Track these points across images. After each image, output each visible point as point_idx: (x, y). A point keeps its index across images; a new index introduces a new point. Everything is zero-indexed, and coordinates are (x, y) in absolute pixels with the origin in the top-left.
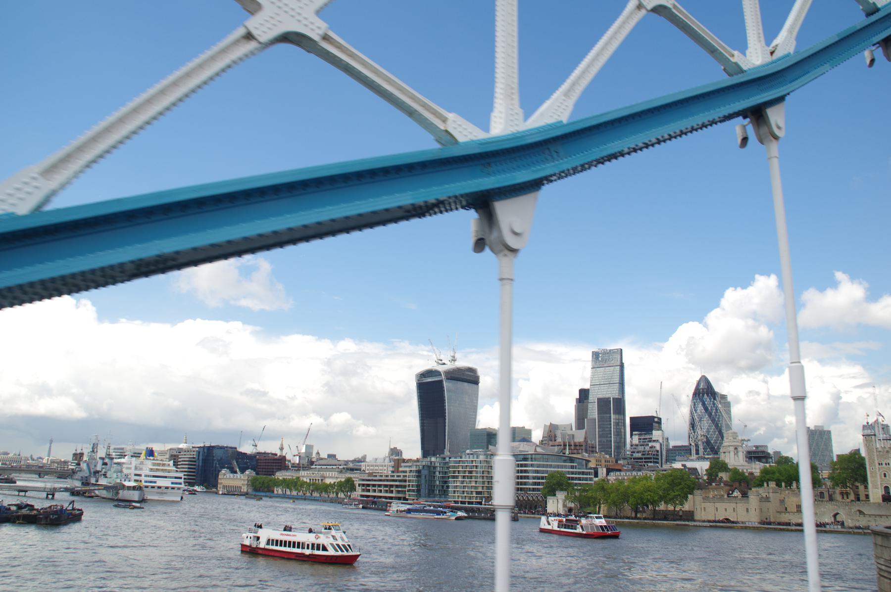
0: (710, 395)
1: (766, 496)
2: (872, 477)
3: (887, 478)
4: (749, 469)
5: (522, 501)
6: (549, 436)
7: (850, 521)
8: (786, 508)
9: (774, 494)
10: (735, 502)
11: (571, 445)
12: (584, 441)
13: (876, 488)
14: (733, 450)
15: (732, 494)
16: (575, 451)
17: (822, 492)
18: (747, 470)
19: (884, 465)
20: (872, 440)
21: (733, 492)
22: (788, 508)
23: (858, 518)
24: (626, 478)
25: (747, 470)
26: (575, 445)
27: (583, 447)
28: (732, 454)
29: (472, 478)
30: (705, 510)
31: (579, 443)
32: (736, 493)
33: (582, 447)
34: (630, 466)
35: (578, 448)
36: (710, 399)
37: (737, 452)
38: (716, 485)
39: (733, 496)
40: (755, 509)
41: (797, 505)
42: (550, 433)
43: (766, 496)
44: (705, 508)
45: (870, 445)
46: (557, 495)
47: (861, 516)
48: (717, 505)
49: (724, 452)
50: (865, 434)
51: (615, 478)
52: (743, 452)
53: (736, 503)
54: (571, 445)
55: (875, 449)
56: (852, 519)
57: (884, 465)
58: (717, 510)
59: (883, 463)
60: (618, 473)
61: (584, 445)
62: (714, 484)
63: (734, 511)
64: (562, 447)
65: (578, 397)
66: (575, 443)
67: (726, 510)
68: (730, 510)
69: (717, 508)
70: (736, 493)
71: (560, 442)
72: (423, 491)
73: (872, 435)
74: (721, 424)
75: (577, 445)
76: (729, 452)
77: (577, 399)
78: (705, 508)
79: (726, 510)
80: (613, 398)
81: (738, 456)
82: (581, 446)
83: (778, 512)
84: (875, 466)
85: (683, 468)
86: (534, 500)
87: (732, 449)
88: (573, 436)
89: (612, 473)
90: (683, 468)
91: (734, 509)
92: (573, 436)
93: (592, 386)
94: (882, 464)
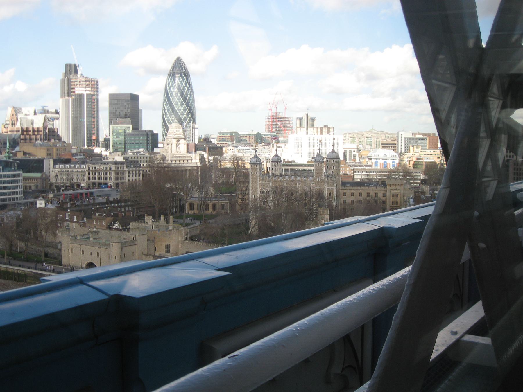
0: (183, 75)
6: (12, 120)
8: (156, 248)
9: (141, 237)
11: (30, 131)
15: (114, 225)
21: (114, 223)
26: (34, 131)
28: (174, 145)
32: (117, 225)
33: (40, 133)
34: (82, 154)
38: (98, 215)
40: (116, 256)
41: (166, 245)
44: (72, 249)
45: (254, 173)
48: (83, 247)
50: (252, 162)
51: (59, 170)
52: (185, 144)
55: (258, 177)
58: (83, 253)
60: (62, 166)
61: (43, 131)
65: (64, 72)
69: (83, 251)
70: (117, 225)
71: (18, 128)
73: (258, 164)
76: (172, 144)
77: (63, 73)
78: (72, 249)
82: (39, 131)
83: (145, 255)
85: (124, 160)
87: (175, 141)
89: (57, 166)
90: (124, 160)
91: (98, 253)
92: (32, 121)
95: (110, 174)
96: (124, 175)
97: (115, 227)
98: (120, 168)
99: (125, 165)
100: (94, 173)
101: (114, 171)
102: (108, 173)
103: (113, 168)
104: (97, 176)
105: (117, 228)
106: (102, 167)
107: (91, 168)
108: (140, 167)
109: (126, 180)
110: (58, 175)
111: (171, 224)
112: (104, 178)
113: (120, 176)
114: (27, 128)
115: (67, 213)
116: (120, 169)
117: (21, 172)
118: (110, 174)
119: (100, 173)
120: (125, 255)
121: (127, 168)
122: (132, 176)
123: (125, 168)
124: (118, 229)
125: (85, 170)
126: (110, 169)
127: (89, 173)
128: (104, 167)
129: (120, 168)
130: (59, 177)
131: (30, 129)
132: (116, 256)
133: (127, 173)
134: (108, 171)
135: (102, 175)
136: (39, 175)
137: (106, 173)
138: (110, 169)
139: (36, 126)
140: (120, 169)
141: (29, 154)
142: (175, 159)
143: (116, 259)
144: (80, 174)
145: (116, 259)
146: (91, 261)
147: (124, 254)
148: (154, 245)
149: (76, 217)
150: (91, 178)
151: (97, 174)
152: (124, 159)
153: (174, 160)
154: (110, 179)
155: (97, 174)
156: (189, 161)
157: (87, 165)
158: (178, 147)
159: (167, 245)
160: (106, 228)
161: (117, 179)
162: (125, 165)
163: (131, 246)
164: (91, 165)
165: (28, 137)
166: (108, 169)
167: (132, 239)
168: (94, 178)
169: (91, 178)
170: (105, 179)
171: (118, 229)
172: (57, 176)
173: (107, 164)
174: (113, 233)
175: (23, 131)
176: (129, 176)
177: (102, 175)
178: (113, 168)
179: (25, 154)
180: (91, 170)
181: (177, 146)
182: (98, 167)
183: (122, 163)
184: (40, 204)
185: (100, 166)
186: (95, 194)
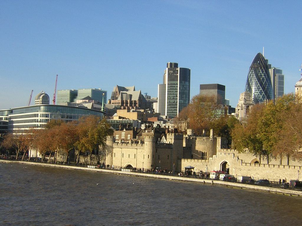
1: (170, 142)
7: (234, 169)
27: (137, 105)
40: (149, 155)
43: (170, 142)
49: (239, 110)
54: (127, 103)
56: (236, 168)
58: (123, 157)
63: (135, 157)
64: (120, 104)
67: (129, 155)
68: (132, 157)
69: (123, 154)
74: (269, 91)
78: (115, 154)
79: (129, 155)
91: (135, 155)
97: (161, 143)
107: (170, 127)
111: (211, 136)
115: (124, 133)
120: (160, 157)
132: (149, 155)
141: (123, 118)
143: (148, 158)
145: (148, 158)
147: (159, 156)
148: (191, 152)
157: (167, 124)
159: (203, 152)
163: (167, 149)
164: (170, 124)
167: (169, 143)
179: (120, 118)
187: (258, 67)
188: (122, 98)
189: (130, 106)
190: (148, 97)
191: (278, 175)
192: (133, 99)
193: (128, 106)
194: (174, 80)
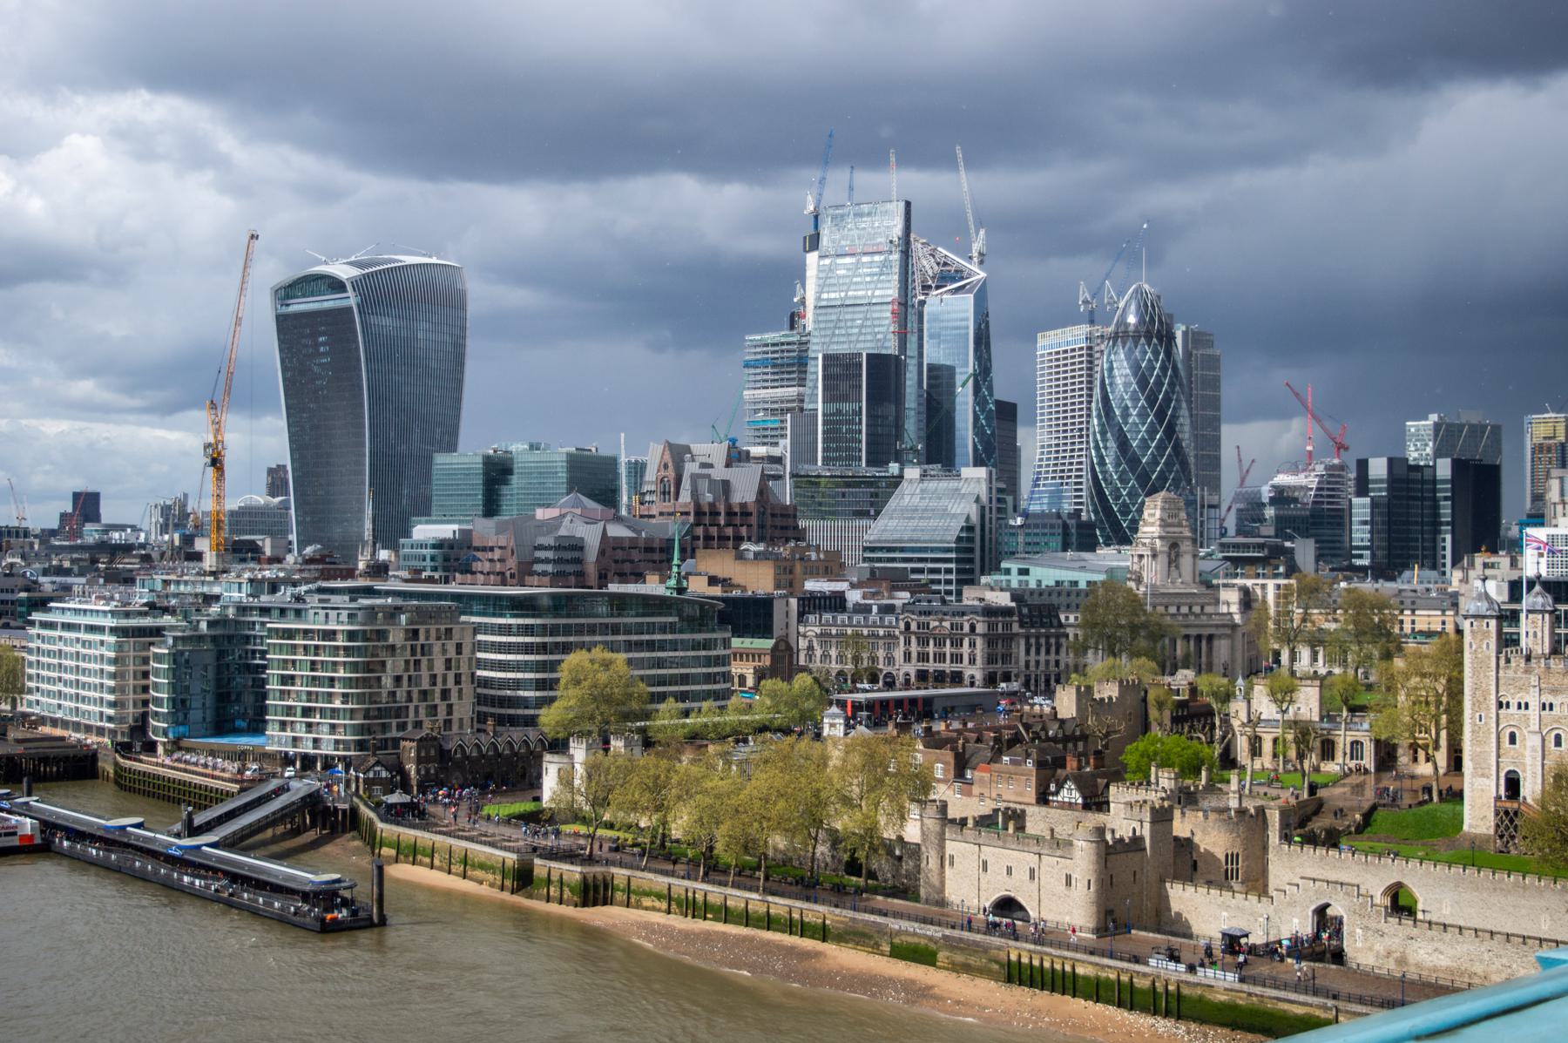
0: (1155, 340)
1: (1134, 830)
2: (1476, 741)
3: (1517, 746)
4: (1209, 604)
5: (478, 759)
6: (662, 481)
7: (1359, 931)
8: (1195, 862)
10: (1036, 849)
11: (718, 514)
12: (757, 501)
13: (1483, 775)
14: (1166, 549)
15: (1057, 793)
16: (729, 531)
17: (1357, 742)
18: (1202, 608)
19: (1513, 709)
20: (1488, 632)
21: (1060, 787)
22: (1199, 864)
23: (1382, 926)
24: (849, 631)
25: (1202, 608)
26: (730, 513)
27: (754, 520)
29: (333, 686)
30: (952, 864)
31: (743, 505)
32: (1070, 793)
35: (738, 520)
36: (1156, 353)
37: (1178, 555)
39: (1060, 799)
41: (1227, 856)
42: (662, 473)
43: (1134, 830)
46: (572, 751)
47: (1390, 919)
48: (989, 852)
51: (818, 630)
53: (1040, 855)
54: (715, 514)
56: (1366, 929)
57: (1513, 709)
58: (985, 869)
59: (1511, 701)
60: (827, 616)
62: (1006, 758)
63: (1032, 877)
64: (691, 519)
66: (729, 507)
67: (1009, 871)
68: (1021, 875)
69: (985, 863)
71: (686, 505)
72: (196, 715)
75: (736, 514)
78: (952, 857)
79: (1009, 871)
80: (868, 355)
81: (1177, 567)
82: (745, 513)
84: (1488, 709)
85: (1013, 604)
86: (516, 754)
88: (726, 485)
89: (811, 618)
90: (1013, 604)
91: (1032, 871)
92: (726, 485)
93: (819, 311)
94: (1508, 703)
95: (972, 645)
96: (1014, 650)
98: (1000, 625)
99: (1016, 618)
100: (923, 641)
101: (984, 635)
102: (966, 642)
103: (980, 628)
104: (931, 649)
105: (1066, 800)
106: (947, 624)
107: (914, 627)
108: (1061, 625)
109: (1017, 662)
110: (815, 644)
112: (952, 655)
113: (1000, 649)
114: (712, 505)
116: (1000, 631)
117: (728, 635)
118: (972, 645)
119: (940, 642)
121: (1021, 626)
122: (1038, 653)
123: (1016, 628)
124: (1070, 803)
125: (897, 633)
126: (973, 628)
127: (908, 642)
128: (952, 625)
129: (1000, 625)
130: (818, 652)
131: (722, 508)
133: (1022, 642)
134: (966, 635)
135: (948, 649)
136: (768, 644)
137: (957, 643)
138: (973, 628)
139: (736, 499)
140: (1000, 631)
142: (1165, 601)
144: (881, 642)
146: (1012, 894)
149: (940, 765)
150: (914, 655)
151: (931, 642)
152: (1012, 600)
153: (1161, 604)
154: (972, 661)
155: (931, 642)
156: (1208, 609)
158: (1173, 569)
160: (1034, 801)
161: (990, 659)
162: (1016, 618)
163: (1130, 855)
165: (714, 531)
166: (967, 628)
168: (923, 657)
169: (914, 655)
170: (957, 658)
171: (1070, 806)
172: (810, 648)
173: (963, 614)
174: (1054, 814)
175: (699, 513)
176: (1028, 652)
177: (948, 649)
178: (980, 628)
179: (713, 581)
180: (915, 633)
181: (1170, 563)
182: (937, 623)
183: (1006, 612)
184: (832, 725)
185: (941, 621)
186: (937, 706)
187: (1140, 337)
188: (695, 494)
189: (727, 525)
190: (739, 453)
191: (1504, 961)
192: (736, 499)
193: (719, 525)
194: (844, 398)
